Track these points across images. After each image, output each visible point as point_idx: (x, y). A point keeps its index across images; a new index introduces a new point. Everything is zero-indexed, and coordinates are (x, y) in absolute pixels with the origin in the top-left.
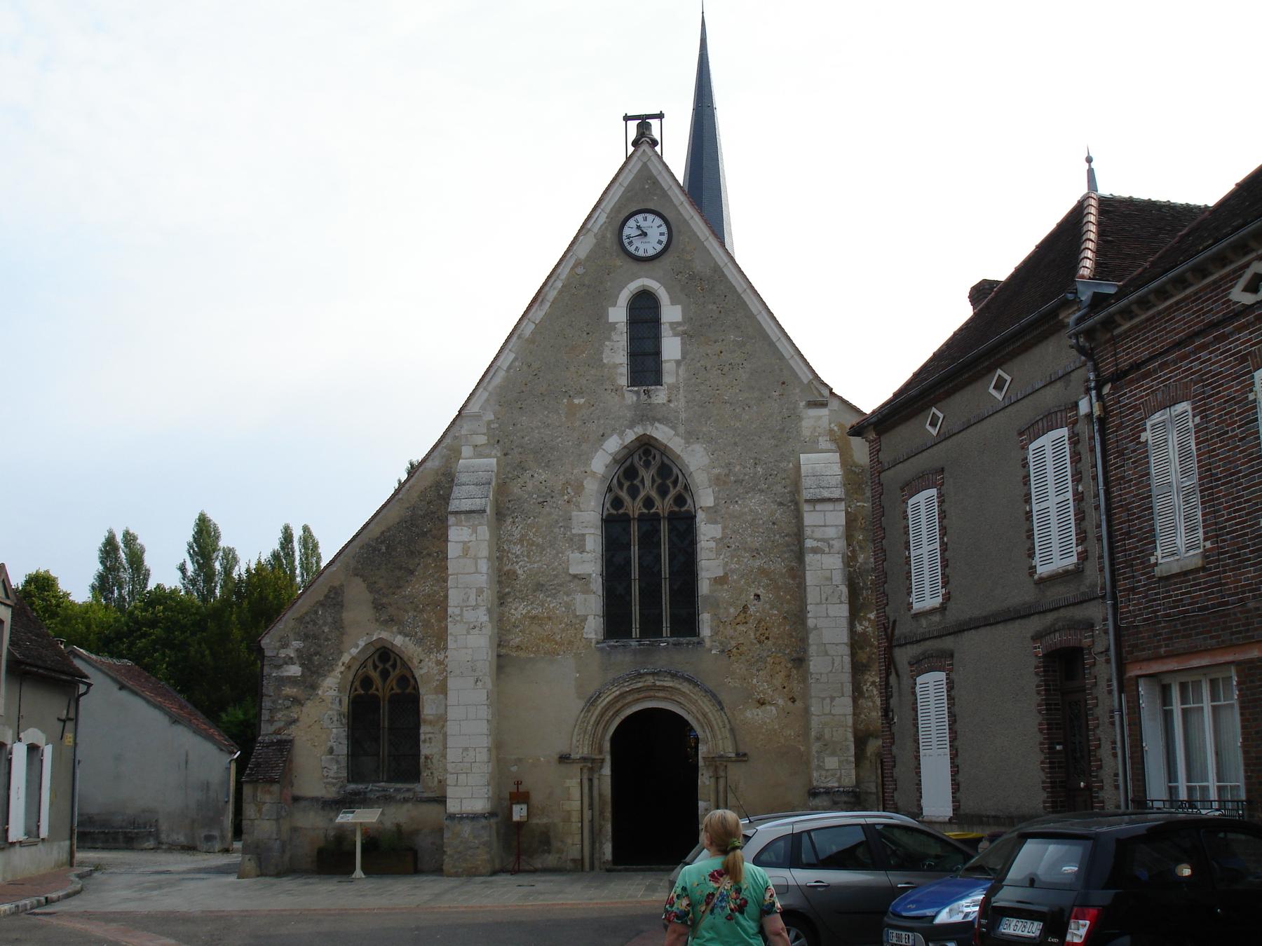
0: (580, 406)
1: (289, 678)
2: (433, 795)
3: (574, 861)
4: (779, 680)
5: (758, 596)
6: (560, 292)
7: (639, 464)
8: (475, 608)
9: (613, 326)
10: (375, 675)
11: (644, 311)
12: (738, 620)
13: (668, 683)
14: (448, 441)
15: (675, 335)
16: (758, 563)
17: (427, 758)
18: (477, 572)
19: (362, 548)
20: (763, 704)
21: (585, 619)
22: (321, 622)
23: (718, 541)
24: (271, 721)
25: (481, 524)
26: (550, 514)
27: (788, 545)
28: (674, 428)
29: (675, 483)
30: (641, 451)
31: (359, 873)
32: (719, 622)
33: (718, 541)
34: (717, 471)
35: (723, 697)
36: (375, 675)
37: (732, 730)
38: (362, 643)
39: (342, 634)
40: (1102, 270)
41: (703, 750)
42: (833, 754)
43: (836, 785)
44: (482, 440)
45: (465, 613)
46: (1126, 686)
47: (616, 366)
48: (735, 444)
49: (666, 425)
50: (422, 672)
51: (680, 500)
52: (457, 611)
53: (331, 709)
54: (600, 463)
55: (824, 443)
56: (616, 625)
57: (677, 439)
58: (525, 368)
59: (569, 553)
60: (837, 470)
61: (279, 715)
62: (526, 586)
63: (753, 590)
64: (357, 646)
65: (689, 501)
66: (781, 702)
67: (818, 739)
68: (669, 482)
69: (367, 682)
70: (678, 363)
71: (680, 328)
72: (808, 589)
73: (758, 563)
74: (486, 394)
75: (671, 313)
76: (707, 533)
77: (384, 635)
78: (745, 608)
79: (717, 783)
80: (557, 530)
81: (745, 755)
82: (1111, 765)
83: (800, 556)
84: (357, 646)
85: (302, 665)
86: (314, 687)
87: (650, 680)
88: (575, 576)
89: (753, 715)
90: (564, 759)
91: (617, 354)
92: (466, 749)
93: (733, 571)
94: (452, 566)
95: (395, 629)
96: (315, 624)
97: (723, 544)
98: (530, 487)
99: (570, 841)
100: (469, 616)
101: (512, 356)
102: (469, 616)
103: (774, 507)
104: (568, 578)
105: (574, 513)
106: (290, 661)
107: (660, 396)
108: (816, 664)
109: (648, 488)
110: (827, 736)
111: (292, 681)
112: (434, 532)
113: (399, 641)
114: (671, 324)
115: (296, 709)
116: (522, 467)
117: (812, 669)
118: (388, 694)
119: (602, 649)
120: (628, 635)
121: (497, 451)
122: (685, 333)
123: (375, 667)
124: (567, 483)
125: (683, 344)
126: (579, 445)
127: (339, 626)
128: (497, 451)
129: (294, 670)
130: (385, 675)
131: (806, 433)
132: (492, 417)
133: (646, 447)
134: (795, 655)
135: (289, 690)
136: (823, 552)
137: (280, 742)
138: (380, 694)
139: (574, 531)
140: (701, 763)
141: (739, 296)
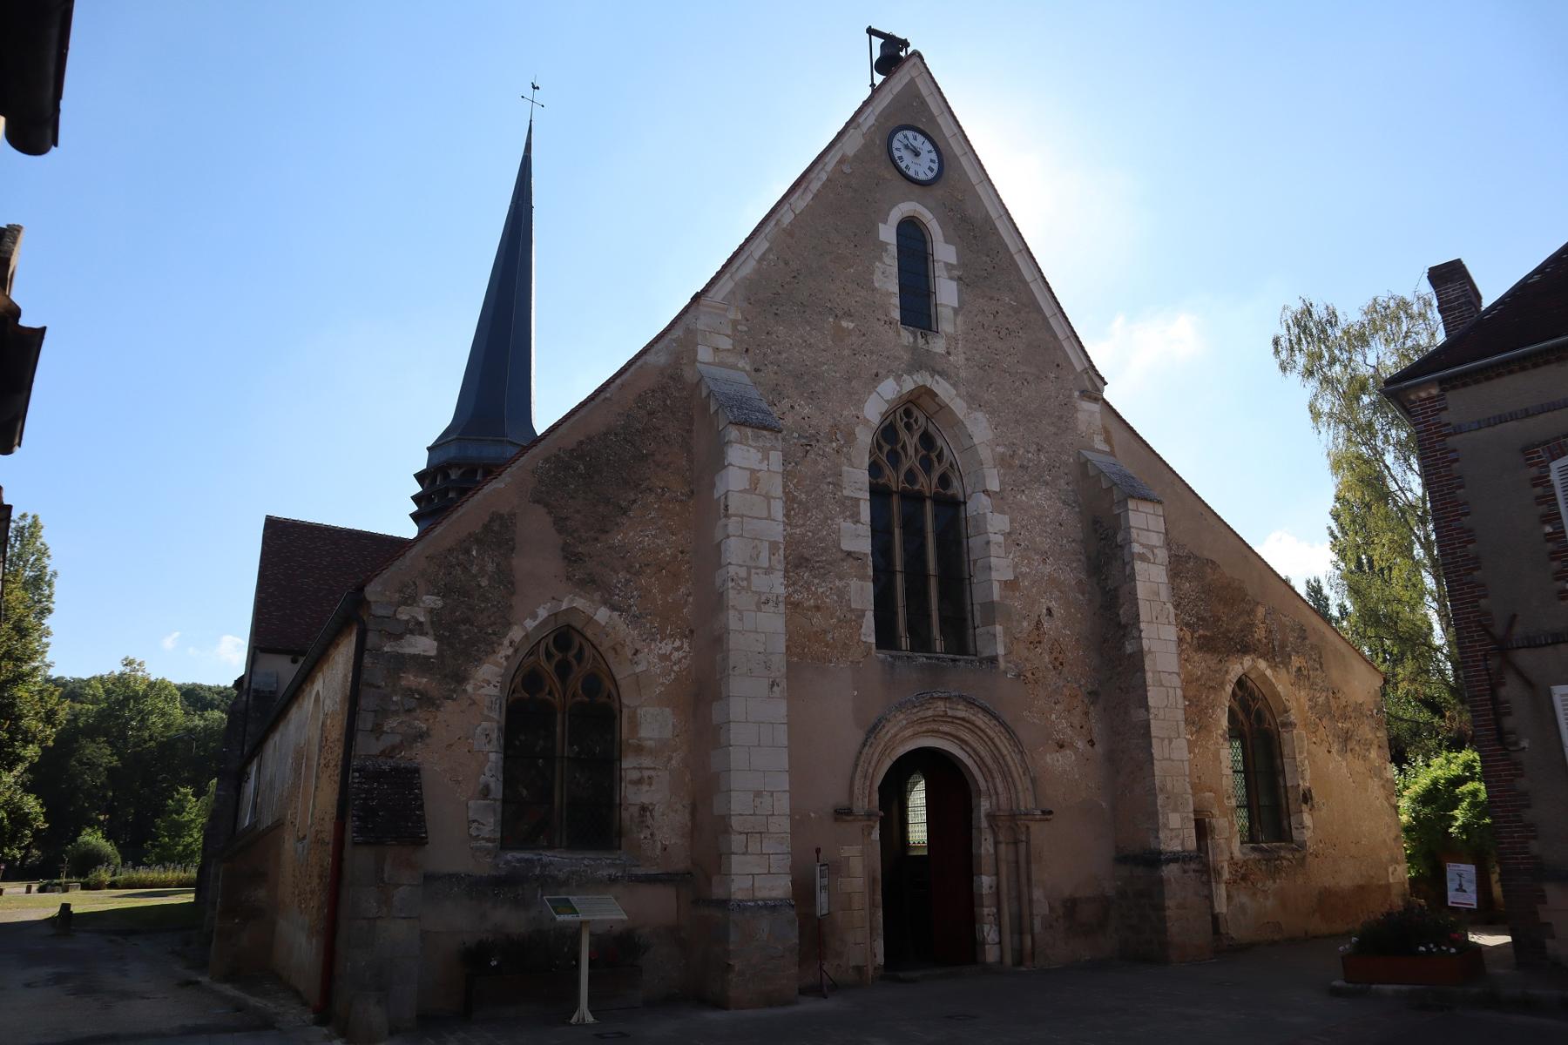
1: (414, 657)
2: (653, 871)
5: (1049, 611)
7: (900, 425)
8: (769, 571)
9: (883, 246)
10: (548, 667)
13: (962, 712)
14: (678, 332)
15: (951, 278)
17: (644, 809)
18: (769, 518)
19: (547, 460)
20: (1062, 746)
21: (862, 614)
22: (474, 570)
23: (1008, 535)
24: (377, 730)
25: (774, 448)
26: (816, 462)
28: (954, 385)
30: (901, 410)
33: (1008, 535)
34: (1000, 449)
36: (548, 667)
37: (1033, 781)
38: (543, 613)
39: (513, 594)
41: (985, 805)
42: (1175, 810)
44: (726, 343)
45: (754, 578)
47: (890, 294)
48: (1017, 421)
51: (944, 481)
52: (743, 573)
53: (488, 719)
54: (874, 410)
57: (958, 400)
58: (782, 265)
61: (391, 723)
63: (1044, 603)
64: (534, 616)
65: (956, 483)
66: (1080, 745)
68: (933, 455)
70: (956, 311)
71: (956, 273)
72: (1141, 603)
73: (1048, 569)
74: (731, 285)
75: (944, 252)
77: (579, 603)
78: (1039, 625)
81: (1051, 812)
84: (534, 616)
85: (438, 638)
86: (461, 678)
88: (849, 554)
90: (842, 814)
91: (887, 279)
92: (758, 794)
93: (1024, 575)
95: (597, 596)
96: (466, 570)
101: (767, 245)
102: (759, 582)
104: (840, 555)
105: (845, 468)
106: (419, 628)
107: (938, 346)
109: (911, 460)
110: (1169, 787)
117: (1151, 702)
119: (883, 662)
121: (744, 363)
122: (960, 278)
123: (549, 655)
125: (960, 291)
126: (849, 380)
127: (506, 580)
129: (424, 645)
130: (563, 670)
131: (1082, 427)
135: (411, 680)
139: (846, 493)
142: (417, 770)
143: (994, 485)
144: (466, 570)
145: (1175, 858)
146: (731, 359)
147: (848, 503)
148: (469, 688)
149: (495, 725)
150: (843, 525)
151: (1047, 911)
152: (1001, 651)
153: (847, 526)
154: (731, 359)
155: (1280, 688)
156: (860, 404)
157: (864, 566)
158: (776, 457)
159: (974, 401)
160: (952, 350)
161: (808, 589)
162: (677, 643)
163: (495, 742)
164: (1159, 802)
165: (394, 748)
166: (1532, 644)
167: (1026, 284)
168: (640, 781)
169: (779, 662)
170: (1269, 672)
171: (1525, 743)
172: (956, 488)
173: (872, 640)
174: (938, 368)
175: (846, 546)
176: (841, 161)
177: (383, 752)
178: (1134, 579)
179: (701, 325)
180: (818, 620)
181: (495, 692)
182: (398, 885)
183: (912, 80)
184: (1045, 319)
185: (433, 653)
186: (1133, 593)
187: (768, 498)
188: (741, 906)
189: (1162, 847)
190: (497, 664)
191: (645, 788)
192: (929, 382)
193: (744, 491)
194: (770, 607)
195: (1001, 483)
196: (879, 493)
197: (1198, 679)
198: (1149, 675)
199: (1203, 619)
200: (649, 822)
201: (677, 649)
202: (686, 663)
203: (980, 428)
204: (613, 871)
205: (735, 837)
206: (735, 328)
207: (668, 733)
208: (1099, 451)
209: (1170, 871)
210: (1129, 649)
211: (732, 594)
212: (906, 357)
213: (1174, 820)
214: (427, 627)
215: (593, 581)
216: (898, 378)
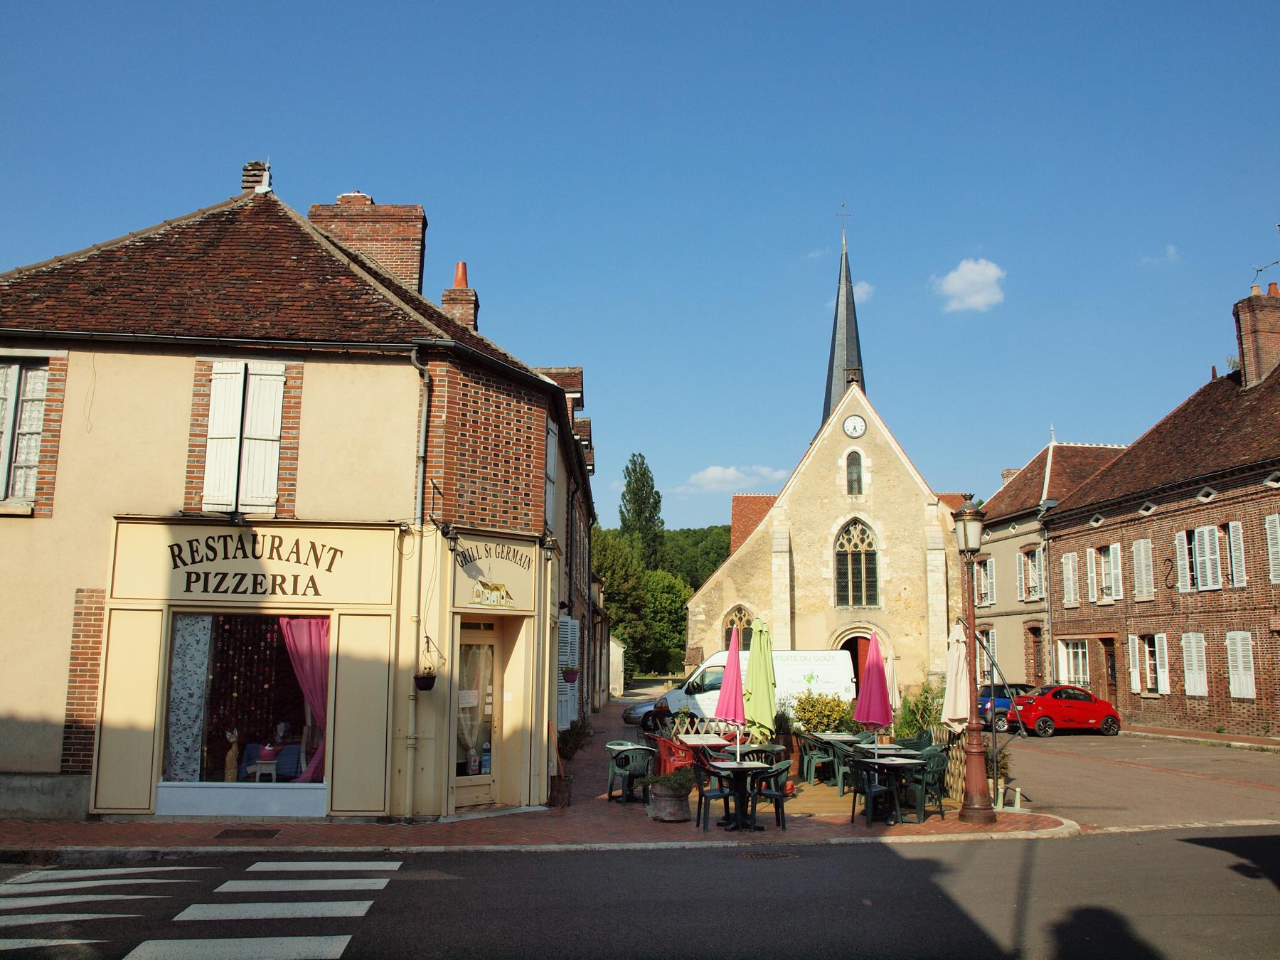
4: (914, 626)
11: (854, 459)
40: (1049, 498)
46: (1054, 642)
51: (870, 545)
55: (936, 522)
56: (842, 599)
60: (941, 534)
66: (916, 635)
75: (866, 462)
76: (882, 562)
82: (1048, 669)
83: (925, 572)
87: (858, 625)
91: (842, 480)
94: (774, 574)
108: (931, 619)
109: (856, 540)
111: (702, 622)
116: (800, 530)
120: (847, 603)
121: (789, 523)
127: (721, 598)
128: (789, 523)
129: (703, 617)
130: (741, 619)
133: (855, 521)
135: (700, 626)
153: (824, 570)
167: (902, 464)
180: (814, 600)
196: (841, 557)
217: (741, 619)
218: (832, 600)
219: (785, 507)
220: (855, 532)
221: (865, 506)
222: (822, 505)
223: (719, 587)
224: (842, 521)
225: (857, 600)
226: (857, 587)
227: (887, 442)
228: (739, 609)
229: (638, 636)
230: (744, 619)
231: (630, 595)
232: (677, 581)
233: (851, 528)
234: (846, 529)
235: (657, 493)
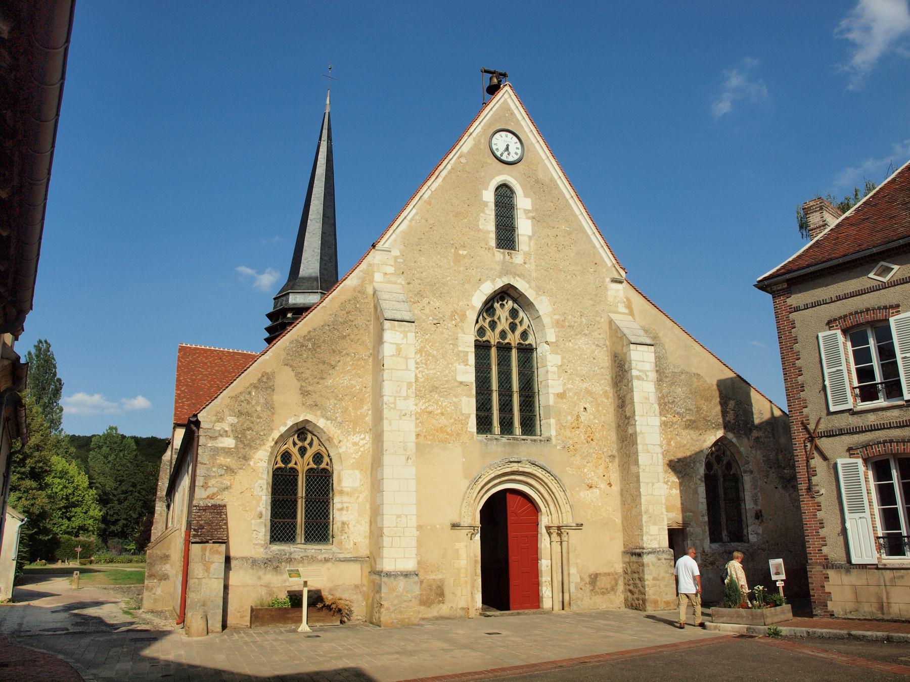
0: (464, 257)
1: (223, 449)
2: (349, 556)
3: (462, 609)
4: (601, 470)
6: (450, 172)
8: (407, 398)
9: (486, 204)
11: (505, 198)
12: (574, 425)
15: (528, 218)
16: (585, 385)
17: (343, 523)
19: (292, 342)
20: (591, 487)
21: (469, 415)
22: (254, 402)
24: (205, 486)
25: (410, 331)
26: (442, 333)
27: (603, 375)
28: (528, 282)
29: (521, 322)
31: (304, 627)
32: (561, 427)
34: (556, 317)
35: (566, 481)
39: (273, 414)
41: (544, 521)
42: (655, 524)
43: (657, 546)
44: (390, 270)
45: (398, 401)
49: (524, 279)
50: (341, 451)
51: (524, 335)
52: (392, 400)
53: (261, 478)
54: (478, 301)
56: (484, 424)
58: (423, 221)
59: (456, 364)
62: (424, 387)
66: (603, 486)
67: (646, 512)
68: (517, 321)
69: (286, 457)
70: (530, 238)
71: (531, 215)
72: (636, 405)
73: (585, 385)
75: (523, 203)
77: (309, 417)
78: (578, 416)
79: (561, 545)
80: (447, 346)
85: (236, 438)
86: (246, 458)
87: (515, 467)
88: (461, 383)
89: (586, 495)
90: (455, 526)
91: (488, 223)
92: (399, 516)
93: (569, 390)
95: (319, 413)
96: (248, 403)
97: (562, 369)
98: (427, 311)
99: (459, 593)
100: (401, 404)
102: (401, 404)
103: (594, 347)
104: (456, 384)
105: (460, 335)
107: (518, 258)
109: (503, 325)
111: (227, 452)
112: (352, 337)
113: (321, 423)
114: (525, 210)
115: (227, 477)
118: (306, 468)
119: (481, 441)
121: (401, 280)
123: (295, 444)
124: (454, 312)
125: (533, 225)
126: (463, 284)
127: (270, 406)
128: (401, 280)
129: (229, 442)
130: (303, 451)
131: (611, 299)
132: (398, 254)
133: (506, 293)
134: (610, 453)
135: (222, 460)
136: (643, 380)
137: (215, 506)
138: (299, 468)
139: (460, 349)
140: (543, 531)
141: (567, 201)
142: (225, 506)
143: (551, 338)
144: (248, 403)
145: (653, 552)
146: (394, 279)
147: (461, 355)
148: (252, 463)
149: (265, 482)
150: (458, 367)
151: (579, 580)
152: (553, 433)
153: (460, 367)
154: (394, 279)
155: (742, 449)
156: (469, 297)
157: (470, 390)
158: (411, 336)
159: (539, 290)
160: (527, 261)
161: (437, 404)
162: (363, 436)
163: (265, 490)
164: (644, 520)
165: (214, 494)
166: (830, 434)
167: (575, 216)
168: (342, 509)
169: (411, 447)
170: (734, 440)
171: (822, 491)
172: (531, 340)
173: (475, 430)
174: (518, 273)
175: (459, 379)
176: (460, 157)
177: (208, 497)
178: (632, 391)
179: (376, 261)
180: (443, 420)
181: (265, 465)
182: (212, 562)
183: (506, 100)
184: (588, 236)
185: (233, 446)
186: (632, 399)
187: (406, 358)
188: (388, 575)
189: (645, 545)
190: (265, 450)
191: (344, 512)
192: (513, 282)
193: (393, 356)
194: (407, 417)
195: (556, 336)
196: (482, 348)
197: (684, 446)
198: (640, 447)
199: (690, 410)
200: (347, 530)
201: (362, 439)
202: (367, 446)
203: (542, 305)
204: (327, 556)
205: (385, 539)
206: (396, 261)
207: (357, 484)
208: (621, 313)
209: (646, 559)
210: (630, 431)
211: (385, 411)
212: (498, 268)
213: (654, 530)
214: (230, 433)
215: (316, 405)
216: (493, 280)
217: (303, 451)
218: (472, 424)
219: (396, 252)
220: (503, 312)
221: (524, 268)
222: (458, 259)
223: (266, 383)
224: (488, 288)
225: (507, 427)
226: (506, 407)
227: (552, 180)
228: (302, 431)
229: (36, 510)
230: (310, 452)
231: (30, 456)
232: (71, 467)
233: (497, 305)
234: (488, 307)
235: (59, 380)
